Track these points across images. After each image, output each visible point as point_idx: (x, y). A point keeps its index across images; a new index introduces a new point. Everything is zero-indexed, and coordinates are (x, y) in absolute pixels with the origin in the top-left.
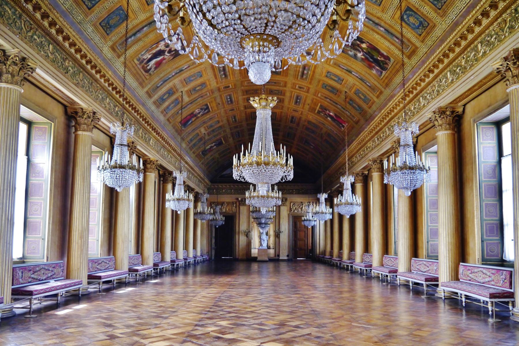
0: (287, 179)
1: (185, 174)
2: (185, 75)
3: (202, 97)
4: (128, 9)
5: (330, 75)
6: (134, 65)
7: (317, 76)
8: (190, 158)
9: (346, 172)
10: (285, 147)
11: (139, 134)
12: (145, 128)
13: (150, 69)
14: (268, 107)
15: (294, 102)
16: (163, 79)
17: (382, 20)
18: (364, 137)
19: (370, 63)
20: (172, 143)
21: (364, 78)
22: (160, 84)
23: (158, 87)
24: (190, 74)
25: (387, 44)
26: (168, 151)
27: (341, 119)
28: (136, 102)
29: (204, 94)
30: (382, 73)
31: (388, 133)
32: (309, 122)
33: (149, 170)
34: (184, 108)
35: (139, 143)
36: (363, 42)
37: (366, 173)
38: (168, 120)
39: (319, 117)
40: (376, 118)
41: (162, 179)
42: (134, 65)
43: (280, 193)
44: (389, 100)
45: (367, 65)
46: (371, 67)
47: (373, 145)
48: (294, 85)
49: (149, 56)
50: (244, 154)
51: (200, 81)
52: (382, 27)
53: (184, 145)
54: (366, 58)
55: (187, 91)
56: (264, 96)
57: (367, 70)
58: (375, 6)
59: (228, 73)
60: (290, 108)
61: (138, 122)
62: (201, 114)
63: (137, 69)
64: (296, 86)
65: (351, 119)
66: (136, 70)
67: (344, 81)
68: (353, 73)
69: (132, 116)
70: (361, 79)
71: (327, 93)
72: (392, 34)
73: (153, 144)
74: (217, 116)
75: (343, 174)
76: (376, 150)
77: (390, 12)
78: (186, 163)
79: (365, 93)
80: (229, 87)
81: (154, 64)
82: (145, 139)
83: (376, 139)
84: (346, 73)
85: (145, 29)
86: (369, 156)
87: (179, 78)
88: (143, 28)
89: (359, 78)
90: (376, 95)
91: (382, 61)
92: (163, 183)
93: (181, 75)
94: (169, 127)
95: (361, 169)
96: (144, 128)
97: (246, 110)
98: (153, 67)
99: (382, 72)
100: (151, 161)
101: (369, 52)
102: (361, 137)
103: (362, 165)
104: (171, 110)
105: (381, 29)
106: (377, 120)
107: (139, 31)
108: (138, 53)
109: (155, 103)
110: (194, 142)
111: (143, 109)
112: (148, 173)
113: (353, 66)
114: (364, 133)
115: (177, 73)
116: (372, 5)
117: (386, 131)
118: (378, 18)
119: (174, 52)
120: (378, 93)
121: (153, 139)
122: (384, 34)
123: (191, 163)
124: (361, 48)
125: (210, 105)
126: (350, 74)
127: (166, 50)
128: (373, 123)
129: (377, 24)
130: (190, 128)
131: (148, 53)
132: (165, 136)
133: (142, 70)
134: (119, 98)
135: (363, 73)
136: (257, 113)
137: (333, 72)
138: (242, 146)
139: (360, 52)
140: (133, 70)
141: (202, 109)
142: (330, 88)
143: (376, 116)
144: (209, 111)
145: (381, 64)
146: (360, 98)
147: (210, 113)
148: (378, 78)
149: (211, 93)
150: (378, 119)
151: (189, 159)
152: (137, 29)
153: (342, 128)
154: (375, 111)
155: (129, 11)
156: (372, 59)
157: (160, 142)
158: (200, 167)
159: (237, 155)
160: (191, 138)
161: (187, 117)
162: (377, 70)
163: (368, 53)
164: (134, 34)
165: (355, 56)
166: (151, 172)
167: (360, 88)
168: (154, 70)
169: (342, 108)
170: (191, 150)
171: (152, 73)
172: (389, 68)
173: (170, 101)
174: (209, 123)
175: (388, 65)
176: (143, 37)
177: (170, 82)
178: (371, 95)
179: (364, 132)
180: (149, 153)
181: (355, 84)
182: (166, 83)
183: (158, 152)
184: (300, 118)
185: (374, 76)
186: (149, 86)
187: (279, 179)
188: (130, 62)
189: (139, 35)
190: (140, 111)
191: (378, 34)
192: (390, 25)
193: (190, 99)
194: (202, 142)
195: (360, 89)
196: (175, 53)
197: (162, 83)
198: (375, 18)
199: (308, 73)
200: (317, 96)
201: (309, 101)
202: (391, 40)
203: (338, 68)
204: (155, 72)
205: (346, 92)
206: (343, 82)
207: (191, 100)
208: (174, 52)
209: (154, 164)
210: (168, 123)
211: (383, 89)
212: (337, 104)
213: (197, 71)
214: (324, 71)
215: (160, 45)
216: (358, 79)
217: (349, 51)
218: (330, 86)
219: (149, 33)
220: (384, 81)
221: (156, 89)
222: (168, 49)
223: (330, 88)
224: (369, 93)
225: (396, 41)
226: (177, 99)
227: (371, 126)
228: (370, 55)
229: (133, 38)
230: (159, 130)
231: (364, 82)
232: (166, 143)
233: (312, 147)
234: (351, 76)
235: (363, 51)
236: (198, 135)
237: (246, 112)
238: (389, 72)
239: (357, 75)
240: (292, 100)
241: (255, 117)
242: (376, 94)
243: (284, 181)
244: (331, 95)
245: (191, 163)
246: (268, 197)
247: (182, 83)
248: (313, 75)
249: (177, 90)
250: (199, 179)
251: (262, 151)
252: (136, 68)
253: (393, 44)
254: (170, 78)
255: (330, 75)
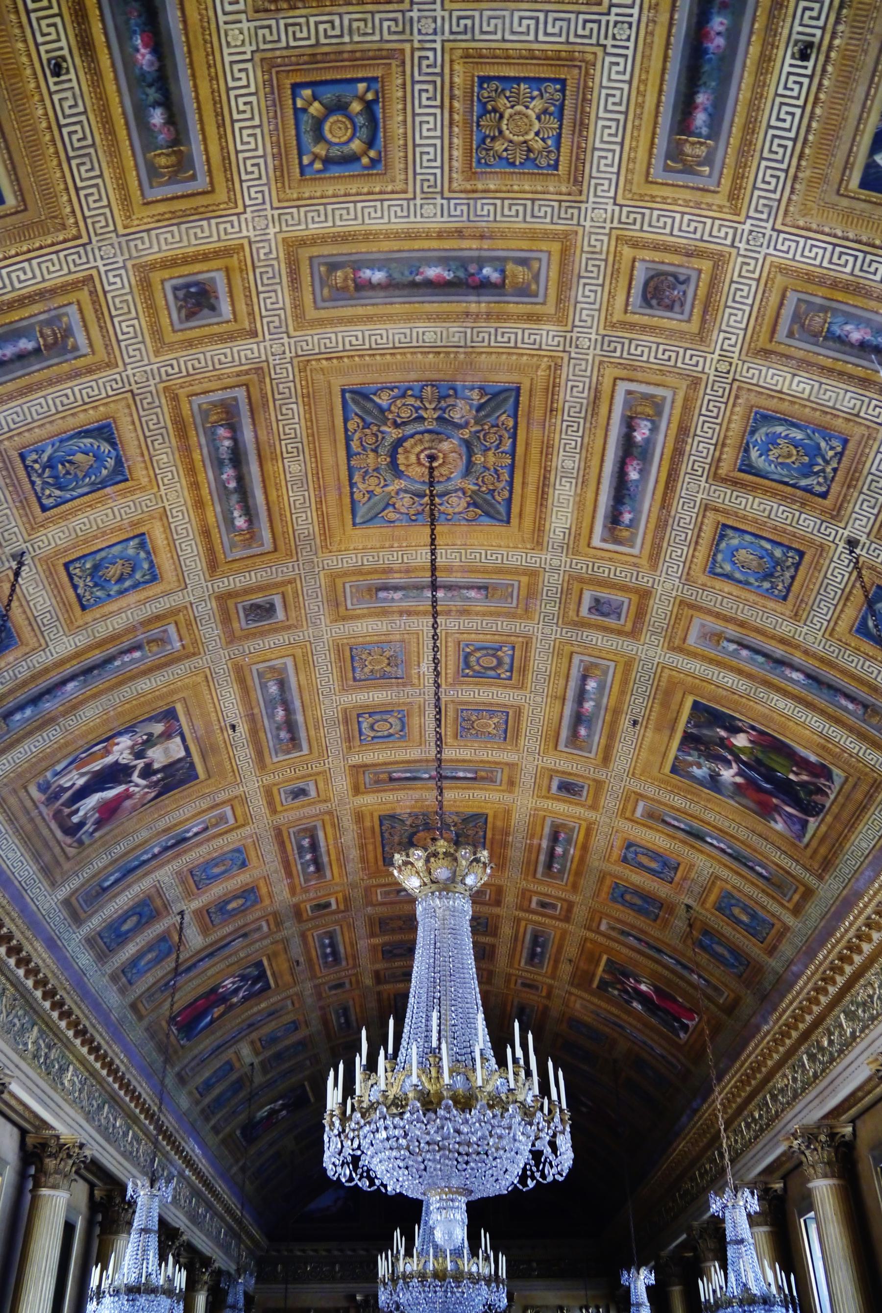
0: (544, 1176)
1: (167, 1192)
2: (195, 856)
3: (245, 935)
4: (10, 601)
5: (636, 853)
6: (29, 804)
7: (594, 861)
8: (200, 1148)
9: (723, 1170)
10: (530, 1037)
11: (26, 1044)
12: (50, 1027)
13: (82, 824)
14: (460, 888)
15: (525, 954)
16: (121, 863)
17: (797, 647)
18: (762, 1054)
19: (763, 797)
20: (144, 1089)
21: (747, 852)
22: (112, 879)
23: (104, 890)
24: (209, 853)
25: (815, 721)
26: (129, 1117)
27: (675, 1001)
28: (24, 927)
29: (253, 926)
30: (804, 825)
31: (849, 1031)
32: (574, 1023)
33: (51, 1180)
34: (188, 969)
35: (17, 1073)
36: (738, 730)
37: (778, 1186)
38: (134, 1007)
39: (604, 1005)
40: (801, 983)
41: (100, 1218)
42: (29, 804)
43: (502, 1260)
44: (839, 915)
45: (752, 805)
46: (766, 811)
47: (795, 1080)
48: (525, 895)
49: (81, 782)
50: (371, 1067)
51: (239, 880)
52: (798, 670)
53: (184, 1102)
54: (750, 781)
55: (198, 913)
56: (442, 846)
57: (754, 821)
58: (771, 604)
59: (325, 859)
60: (513, 978)
61: (27, 1001)
62: (241, 995)
63: (38, 820)
64: (530, 902)
65: (709, 998)
66: (32, 820)
67: (681, 868)
68: (709, 840)
69: (7, 979)
70: (736, 857)
71: (629, 916)
72: (830, 687)
73: (74, 1084)
74: (290, 1007)
75: (717, 1183)
76: (814, 1093)
77: (822, 615)
78: (189, 1162)
79: (751, 903)
80: (328, 905)
81: (93, 808)
82: (48, 1067)
83: (805, 1057)
84: (684, 842)
85: (70, 686)
86: (785, 1121)
87: (176, 865)
88: (64, 682)
89: (730, 855)
90: (790, 905)
91: (803, 784)
92: (103, 1232)
93: (179, 855)
94: (136, 1034)
95: (760, 1174)
96: (47, 1025)
97: (382, 987)
98: (92, 820)
99: (807, 821)
100: (61, 1146)
101: (758, 761)
102: (749, 1056)
103: (767, 1154)
104: (146, 972)
105: (796, 675)
106: (802, 989)
107: (49, 691)
108: (44, 764)
109: (90, 942)
110: (216, 1092)
111: (45, 956)
112: (44, 1191)
113: (710, 817)
114: (760, 1042)
115: (166, 849)
116: (761, 601)
117: (841, 1026)
118: (783, 641)
119: (159, 776)
120: (796, 897)
121: (75, 1070)
122: (804, 693)
123: (204, 1165)
124: (731, 749)
125: (271, 965)
126: (699, 844)
127: (135, 767)
128: (789, 1005)
129: (781, 662)
130: (207, 1041)
131: (78, 768)
132: (117, 1061)
133: (54, 825)
134: (23, 979)
135: (743, 834)
136: (419, 909)
137: (644, 843)
138: (364, 1033)
139: (728, 763)
140: (24, 820)
141: (243, 978)
142: (639, 902)
143: (798, 976)
144: (267, 987)
145: (802, 795)
146: (739, 922)
147: (270, 992)
148: (794, 845)
149: (272, 926)
150: (806, 984)
151: (197, 1151)
152: (43, 684)
153: (682, 1035)
154: (791, 962)
155: (15, 604)
156: (767, 783)
157: (101, 1082)
158: (223, 1175)
159: (341, 1067)
160: (209, 1079)
161: (195, 1001)
162: (790, 815)
163: (756, 765)
164: (35, 701)
165: (714, 781)
166: (54, 1187)
167: (734, 887)
168: (95, 830)
169: (679, 962)
170: (207, 1119)
171: (87, 840)
172: (828, 805)
173: (143, 943)
174: (266, 1030)
175: (827, 795)
176: (64, 714)
177: (146, 875)
178: (774, 907)
179: (758, 1037)
180: (56, 1115)
181: (717, 877)
182: (130, 878)
183: (89, 1117)
184: (546, 1008)
185: (779, 842)
186: (75, 883)
187: (514, 1176)
188: (15, 791)
189: (48, 706)
190: (36, 960)
191: (785, 693)
192: (822, 660)
193: (209, 940)
194: (242, 1095)
195: (735, 893)
196: (162, 779)
197: (117, 875)
198: (773, 643)
199: (566, 852)
200: (598, 932)
201: (571, 950)
202: (831, 709)
203: (661, 826)
204: (97, 835)
205: (688, 907)
206: (679, 874)
207: (211, 945)
208: (159, 776)
209: (69, 1156)
210: (131, 1016)
211: (812, 881)
212: (659, 951)
213: (231, 847)
214: (618, 843)
215: (116, 748)
216: (726, 859)
217: (691, 765)
218: (638, 892)
219: (82, 703)
220: (815, 851)
221: (98, 895)
222: (140, 763)
223: (639, 902)
224: (765, 900)
225: (845, 709)
226: (163, 938)
227: (784, 1011)
228: (763, 770)
229: (28, 712)
230: (98, 1038)
231: (745, 865)
232: (120, 1088)
233: (584, 1110)
234: (701, 852)
235: (738, 760)
236: (229, 1067)
237: (379, 993)
238: (829, 819)
239: (722, 846)
240: (519, 948)
241: (410, 923)
242: (789, 901)
243: (531, 1184)
244: (641, 922)
245: (204, 1165)
246: (458, 1276)
247: (183, 882)
248: (582, 859)
249: (166, 906)
250: (230, 1228)
251: (444, 1046)
252: (34, 813)
253: (838, 721)
254: (145, 862)
255: (636, 853)
